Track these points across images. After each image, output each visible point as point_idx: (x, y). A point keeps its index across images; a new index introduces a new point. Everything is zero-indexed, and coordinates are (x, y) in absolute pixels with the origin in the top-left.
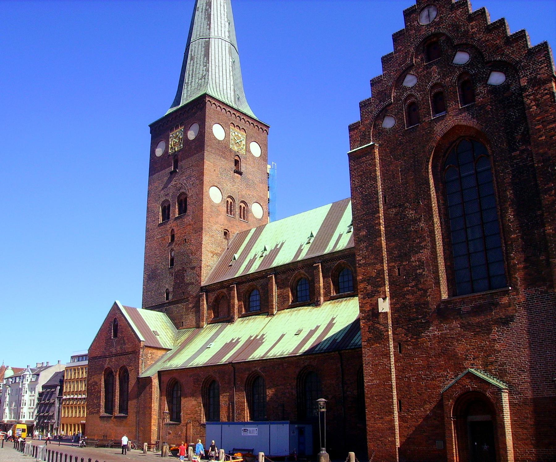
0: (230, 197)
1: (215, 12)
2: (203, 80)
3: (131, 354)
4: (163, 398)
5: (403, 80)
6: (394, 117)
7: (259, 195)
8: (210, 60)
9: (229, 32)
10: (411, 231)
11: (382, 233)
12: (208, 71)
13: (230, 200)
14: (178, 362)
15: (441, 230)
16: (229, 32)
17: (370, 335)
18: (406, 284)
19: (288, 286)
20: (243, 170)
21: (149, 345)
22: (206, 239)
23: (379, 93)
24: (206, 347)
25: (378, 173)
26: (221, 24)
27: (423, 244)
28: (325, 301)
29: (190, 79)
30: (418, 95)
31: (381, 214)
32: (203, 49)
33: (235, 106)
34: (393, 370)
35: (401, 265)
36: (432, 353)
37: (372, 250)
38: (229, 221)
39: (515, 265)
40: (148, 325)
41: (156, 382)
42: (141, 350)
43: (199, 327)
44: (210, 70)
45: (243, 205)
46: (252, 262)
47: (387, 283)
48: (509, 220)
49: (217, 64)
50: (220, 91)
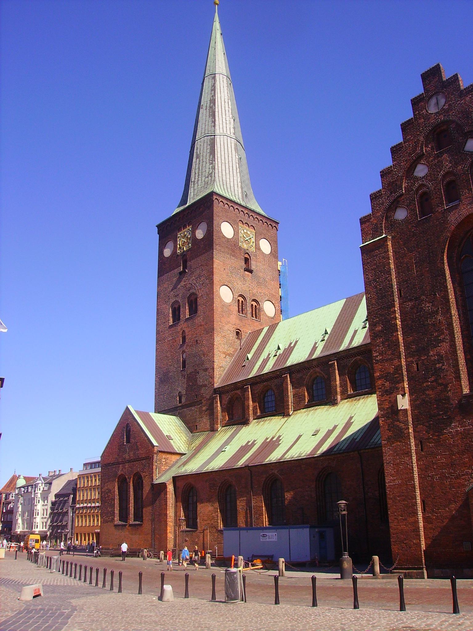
0: (241, 296)
1: (220, 109)
2: (210, 178)
3: (144, 460)
4: (178, 504)
5: (414, 170)
6: (406, 208)
7: (271, 292)
8: (216, 157)
9: (234, 128)
10: (429, 324)
11: (398, 327)
12: (215, 168)
13: (241, 299)
14: (193, 467)
15: (460, 323)
16: (234, 128)
17: (390, 434)
20: (253, 267)
21: (163, 450)
22: (217, 339)
23: (390, 184)
24: (220, 450)
25: (392, 266)
26: (226, 121)
27: (441, 337)
28: (342, 399)
29: (197, 177)
30: (430, 184)
31: (397, 308)
32: (209, 147)
33: (243, 203)
34: (415, 469)
35: (419, 360)
36: (455, 450)
37: (388, 346)
38: (241, 320)
40: (161, 429)
41: (170, 488)
42: (155, 456)
43: (213, 430)
44: (216, 167)
45: (254, 304)
46: (265, 361)
47: (406, 378)
49: (223, 161)
50: (227, 188)
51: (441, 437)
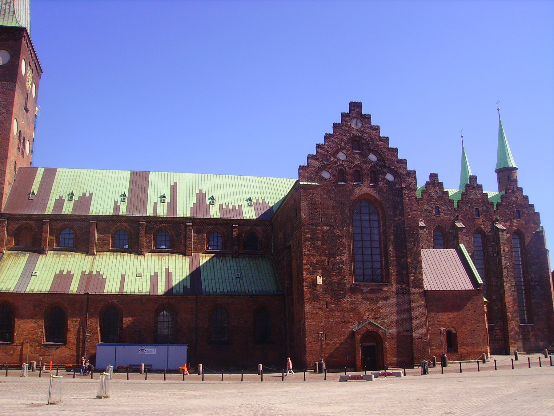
18: (333, 271)
19: (110, 233)
27: (344, 251)
35: (330, 260)
36: (346, 310)
37: (314, 247)
39: (392, 273)
46: (60, 203)
48: (391, 250)
51: (339, 302)
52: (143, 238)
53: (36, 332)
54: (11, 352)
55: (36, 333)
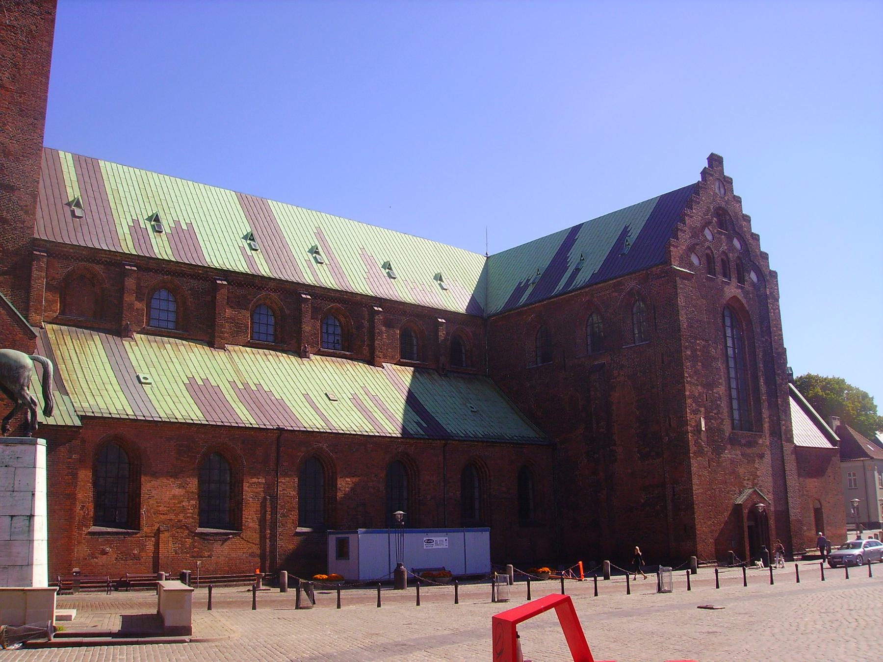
19: (247, 310)
52: (308, 326)
53: (183, 506)
54: (136, 552)
55: (184, 510)
